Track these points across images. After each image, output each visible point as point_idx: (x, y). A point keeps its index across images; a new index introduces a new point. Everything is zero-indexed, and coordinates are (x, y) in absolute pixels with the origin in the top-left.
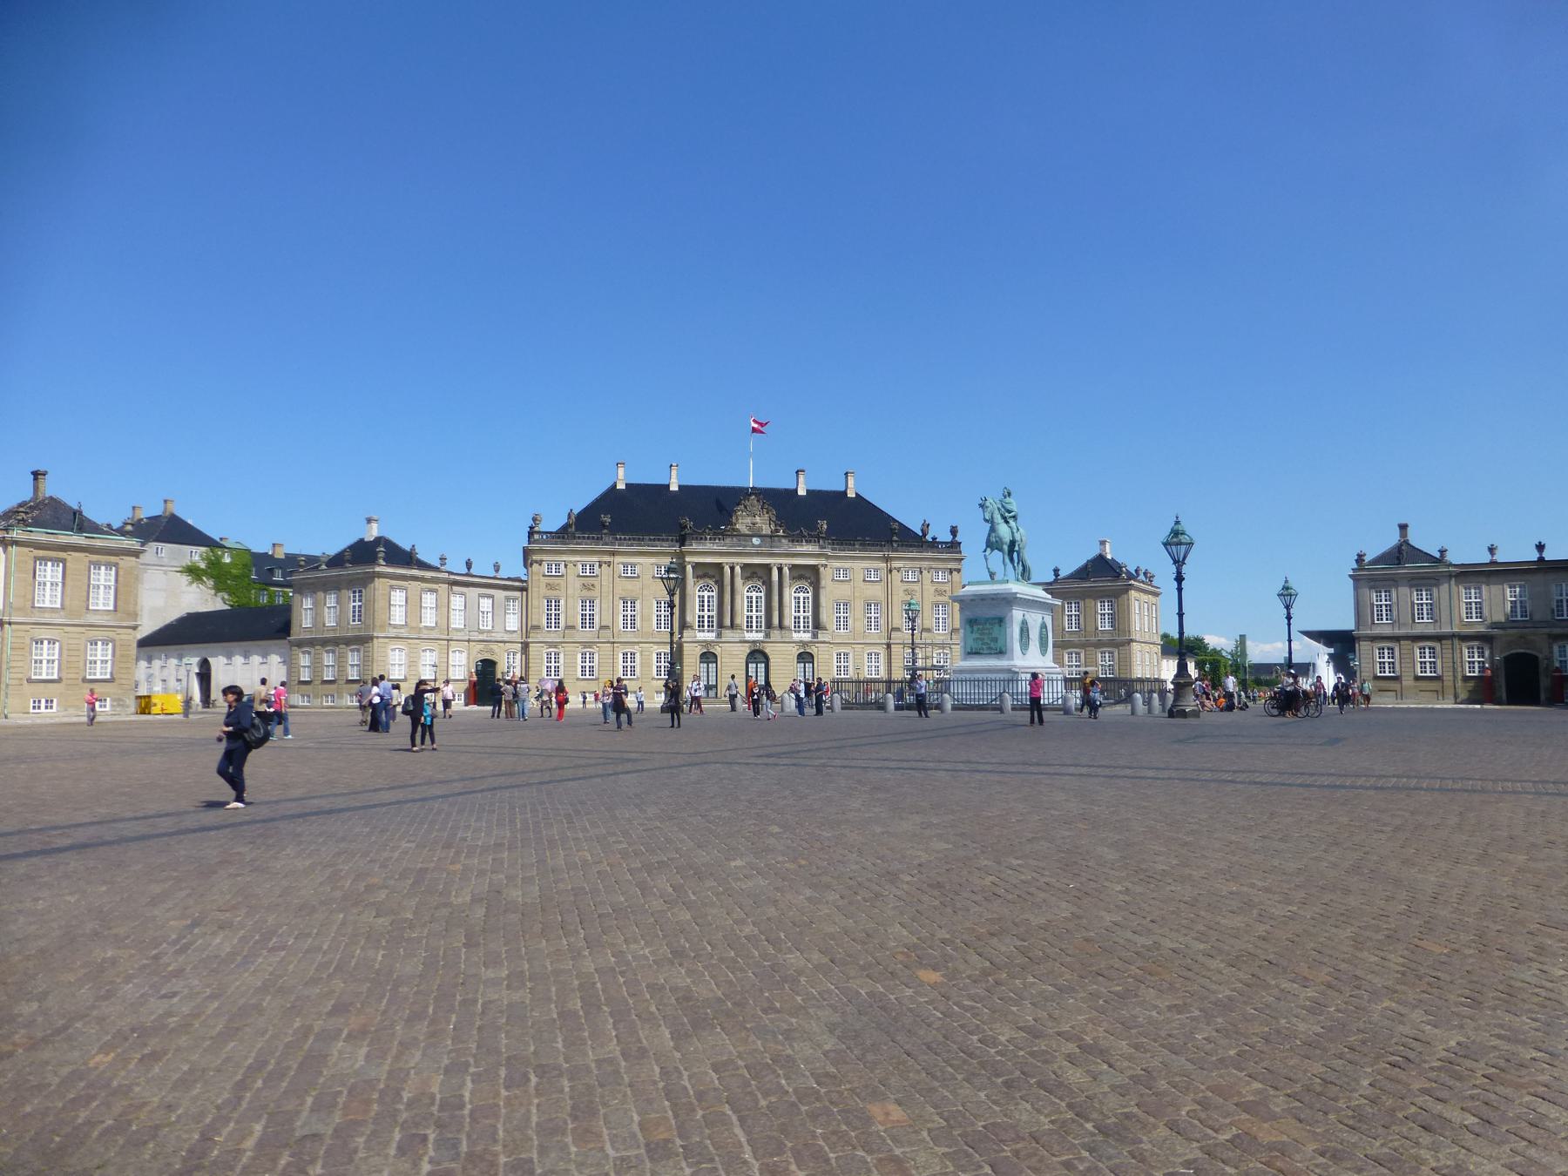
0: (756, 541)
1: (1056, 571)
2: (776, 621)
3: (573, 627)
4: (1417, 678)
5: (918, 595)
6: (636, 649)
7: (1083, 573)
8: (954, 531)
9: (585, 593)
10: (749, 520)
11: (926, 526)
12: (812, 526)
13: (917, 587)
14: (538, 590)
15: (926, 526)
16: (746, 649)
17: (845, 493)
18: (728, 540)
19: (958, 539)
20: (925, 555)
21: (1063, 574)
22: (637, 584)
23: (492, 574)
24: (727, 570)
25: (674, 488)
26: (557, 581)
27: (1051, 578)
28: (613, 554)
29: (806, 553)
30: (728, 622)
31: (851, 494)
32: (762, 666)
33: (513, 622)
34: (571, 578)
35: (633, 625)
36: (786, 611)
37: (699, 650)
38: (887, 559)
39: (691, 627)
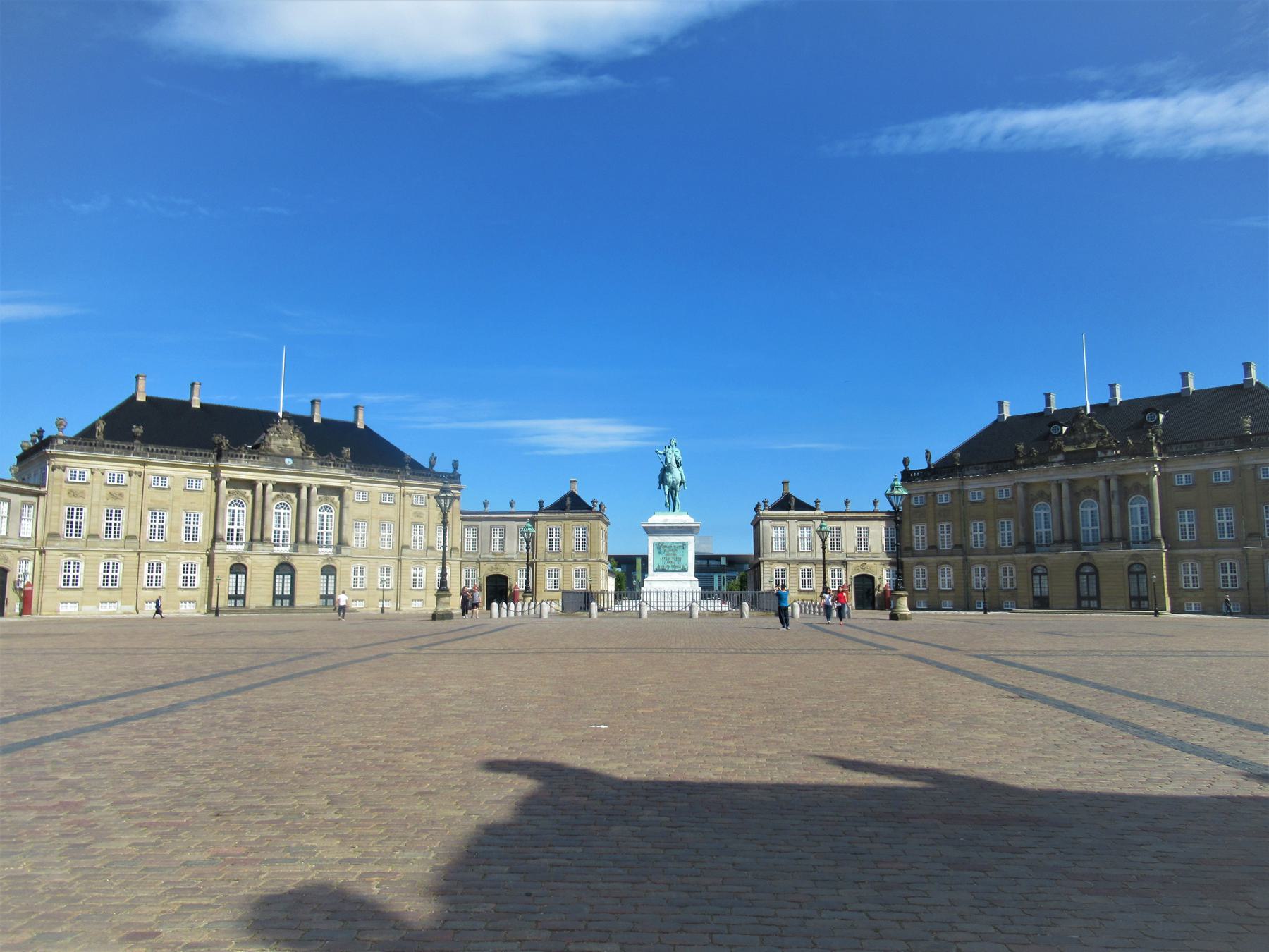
0: (288, 461)
1: (541, 503)
2: (302, 536)
3: (97, 536)
4: (800, 591)
5: (425, 517)
6: (162, 560)
7: (560, 506)
8: (455, 465)
9: (111, 502)
10: (280, 442)
11: (433, 460)
12: (339, 454)
13: (424, 511)
15: (433, 460)
16: (275, 562)
18: (262, 459)
19: (459, 471)
21: (546, 505)
22: (167, 496)
24: (260, 487)
26: (80, 488)
27: (537, 508)
28: (144, 464)
29: (334, 476)
32: (288, 578)
34: (97, 487)
35: (161, 536)
36: (312, 527)
37: (229, 562)
38: (400, 485)
39: (222, 539)
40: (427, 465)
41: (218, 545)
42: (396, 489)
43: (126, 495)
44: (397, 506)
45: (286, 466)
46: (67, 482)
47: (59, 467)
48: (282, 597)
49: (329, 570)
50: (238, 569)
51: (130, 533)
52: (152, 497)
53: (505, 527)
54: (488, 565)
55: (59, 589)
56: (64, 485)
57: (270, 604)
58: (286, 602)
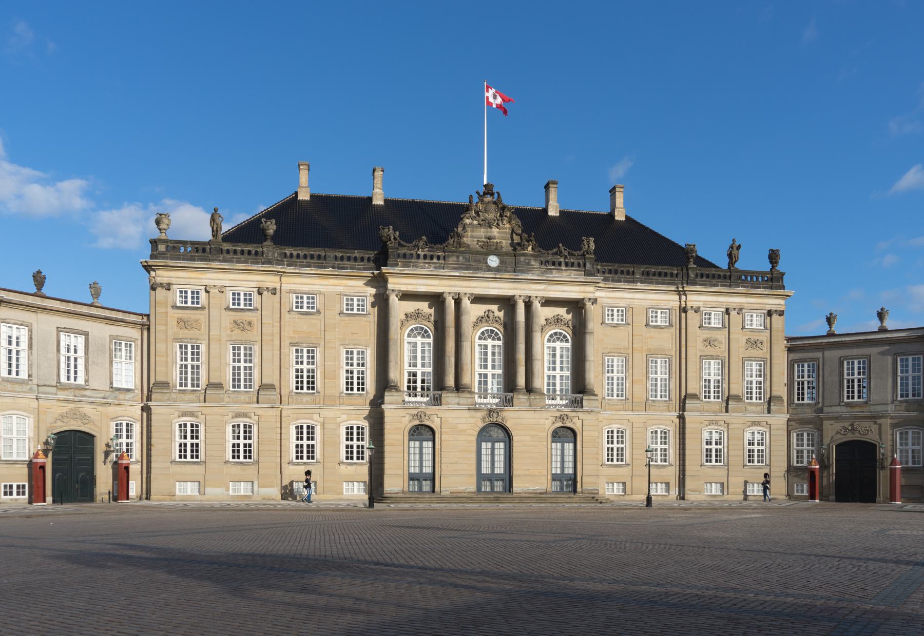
0: (493, 261)
2: (521, 381)
3: (219, 386)
8: (773, 257)
9: (237, 334)
10: (482, 233)
14: (166, 326)
17: (611, 215)
18: (452, 260)
19: (780, 268)
20: (737, 290)
23: (89, 300)
25: (378, 201)
30: (450, 381)
31: (620, 216)
32: (500, 447)
33: (127, 374)
34: (214, 312)
35: (311, 385)
37: (407, 423)
39: (396, 388)
40: (723, 263)
41: (389, 397)
42: (672, 300)
43: (257, 324)
44: (674, 331)
45: (490, 269)
46: (175, 307)
47: (161, 285)
48: (491, 478)
49: (565, 434)
50: (422, 432)
51: (266, 381)
52: (295, 326)
53: (869, 357)
54: (838, 426)
55: (173, 462)
56: (171, 312)
57: (473, 488)
58: (499, 486)
